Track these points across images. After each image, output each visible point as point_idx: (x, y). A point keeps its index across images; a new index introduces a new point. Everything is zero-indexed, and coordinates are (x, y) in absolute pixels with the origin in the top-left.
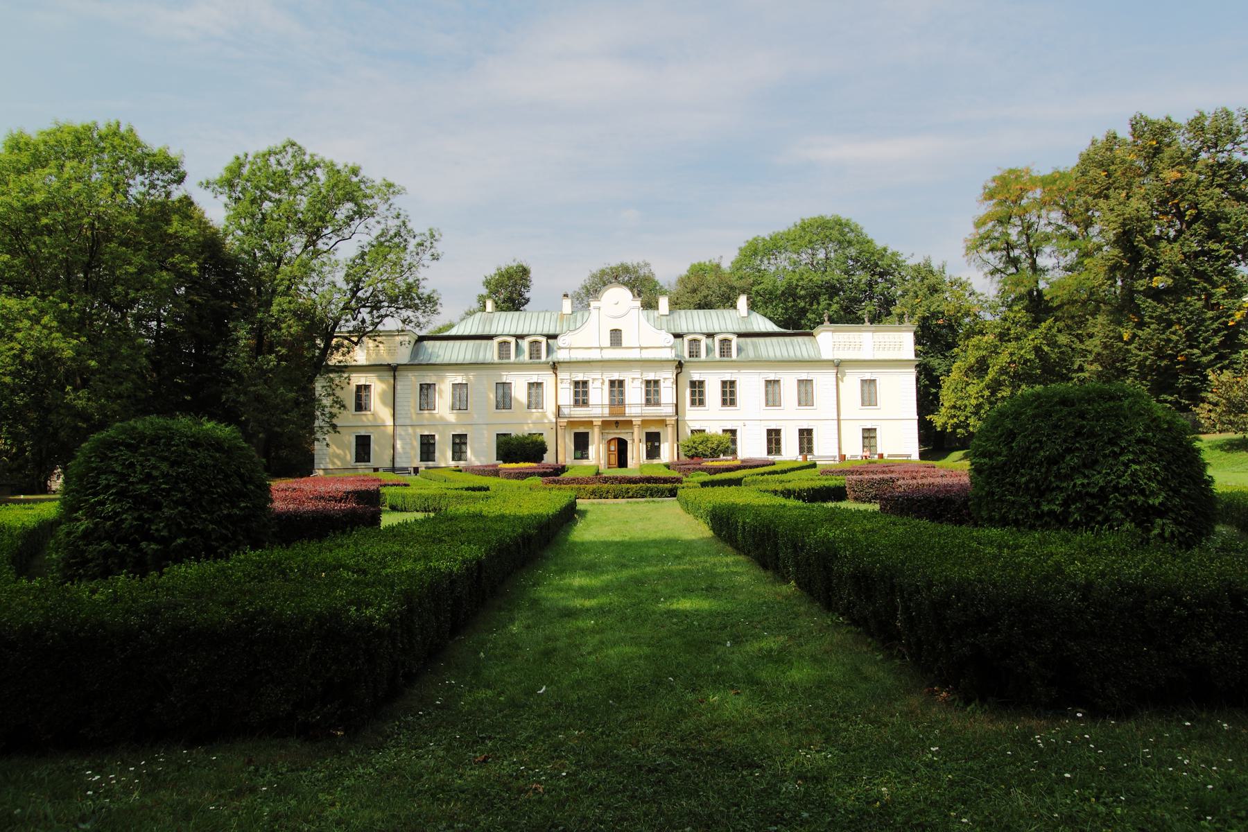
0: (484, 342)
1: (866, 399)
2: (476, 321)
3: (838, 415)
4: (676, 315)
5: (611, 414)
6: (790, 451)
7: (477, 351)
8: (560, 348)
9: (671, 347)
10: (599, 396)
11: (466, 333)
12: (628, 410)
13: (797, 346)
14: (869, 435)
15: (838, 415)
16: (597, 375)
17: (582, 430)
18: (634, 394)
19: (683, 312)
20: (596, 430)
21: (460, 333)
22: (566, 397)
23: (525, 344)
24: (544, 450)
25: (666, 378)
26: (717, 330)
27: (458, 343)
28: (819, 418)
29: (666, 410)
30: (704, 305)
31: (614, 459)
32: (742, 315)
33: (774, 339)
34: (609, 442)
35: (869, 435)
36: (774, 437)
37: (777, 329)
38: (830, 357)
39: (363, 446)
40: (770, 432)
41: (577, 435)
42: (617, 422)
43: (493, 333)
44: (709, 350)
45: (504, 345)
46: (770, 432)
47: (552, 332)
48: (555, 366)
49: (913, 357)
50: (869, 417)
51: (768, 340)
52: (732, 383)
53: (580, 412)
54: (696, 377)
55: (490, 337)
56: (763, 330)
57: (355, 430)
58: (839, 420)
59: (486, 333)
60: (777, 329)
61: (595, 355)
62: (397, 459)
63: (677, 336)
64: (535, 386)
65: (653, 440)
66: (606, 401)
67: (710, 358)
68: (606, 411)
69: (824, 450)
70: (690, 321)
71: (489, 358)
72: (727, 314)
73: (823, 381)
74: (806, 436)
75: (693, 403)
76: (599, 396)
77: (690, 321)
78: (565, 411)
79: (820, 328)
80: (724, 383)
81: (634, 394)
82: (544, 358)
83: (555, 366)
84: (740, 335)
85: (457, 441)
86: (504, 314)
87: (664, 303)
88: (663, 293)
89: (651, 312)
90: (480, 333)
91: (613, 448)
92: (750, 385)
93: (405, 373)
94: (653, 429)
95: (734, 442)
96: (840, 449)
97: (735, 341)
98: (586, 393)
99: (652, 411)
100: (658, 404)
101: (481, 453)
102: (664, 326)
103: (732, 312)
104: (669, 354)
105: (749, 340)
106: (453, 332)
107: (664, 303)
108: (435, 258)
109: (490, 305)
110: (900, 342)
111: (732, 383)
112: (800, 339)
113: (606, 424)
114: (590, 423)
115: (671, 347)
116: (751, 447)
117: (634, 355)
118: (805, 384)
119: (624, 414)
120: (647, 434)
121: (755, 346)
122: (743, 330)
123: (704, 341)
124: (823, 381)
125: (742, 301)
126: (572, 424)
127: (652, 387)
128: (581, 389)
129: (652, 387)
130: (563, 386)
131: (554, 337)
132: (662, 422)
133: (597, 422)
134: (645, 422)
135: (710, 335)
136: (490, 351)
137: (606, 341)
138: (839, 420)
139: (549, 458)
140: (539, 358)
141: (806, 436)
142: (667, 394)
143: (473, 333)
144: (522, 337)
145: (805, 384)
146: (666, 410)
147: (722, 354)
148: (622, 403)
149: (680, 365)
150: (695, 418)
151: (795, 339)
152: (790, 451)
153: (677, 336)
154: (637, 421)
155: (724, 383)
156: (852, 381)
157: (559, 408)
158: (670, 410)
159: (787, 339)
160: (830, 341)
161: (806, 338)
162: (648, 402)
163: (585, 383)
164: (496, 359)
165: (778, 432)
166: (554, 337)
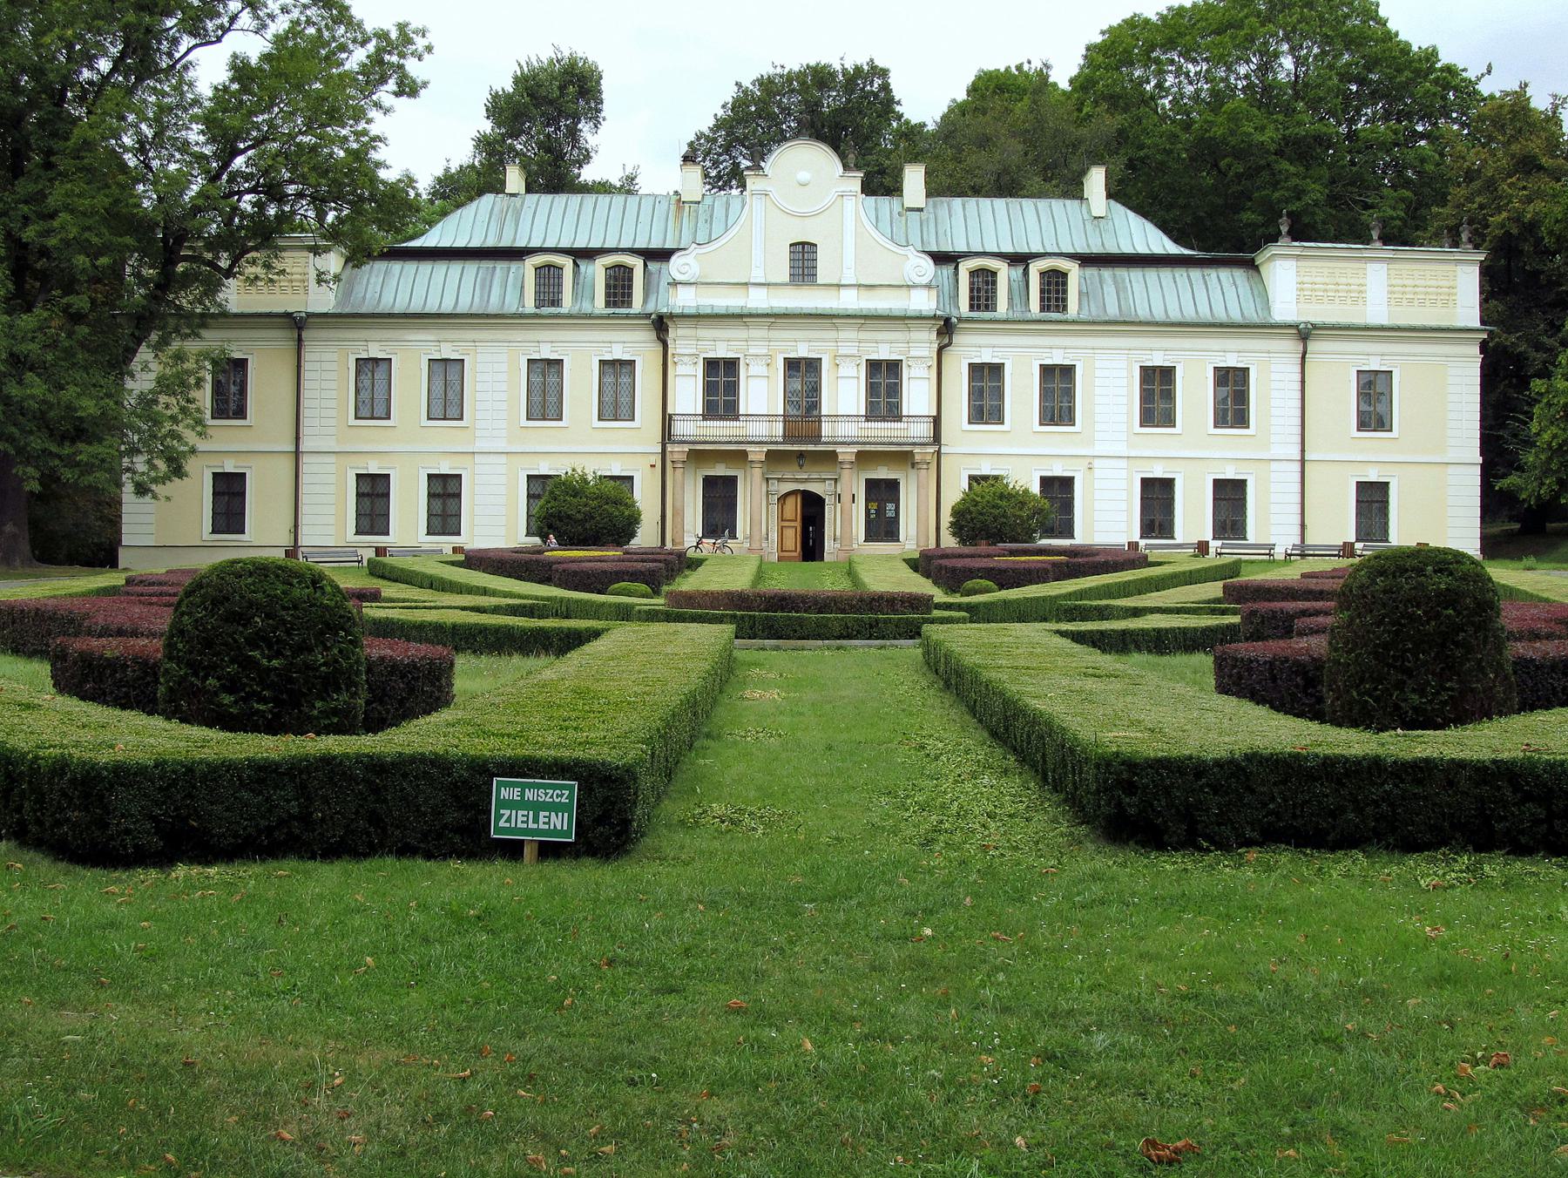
0: (501, 266)
2: (483, 216)
3: (1303, 451)
4: (943, 212)
5: (788, 437)
7: (487, 287)
8: (675, 284)
9: (928, 286)
10: (762, 394)
11: (461, 243)
12: (826, 429)
13: (1218, 291)
14: (1372, 498)
15: (1303, 451)
17: (720, 470)
18: (843, 395)
19: (957, 202)
20: (757, 472)
21: (446, 243)
22: (688, 394)
23: (596, 271)
25: (916, 350)
26: (1036, 248)
27: (441, 268)
28: (1262, 454)
30: (1006, 186)
31: (793, 539)
32: (1097, 216)
33: (1166, 274)
35: (1372, 498)
36: (1157, 497)
37: (1172, 248)
38: (1291, 318)
39: (230, 496)
41: (709, 482)
42: (801, 455)
43: (521, 243)
45: (548, 279)
47: (655, 244)
48: (661, 325)
49: (1477, 324)
50: (1373, 457)
51: (1151, 274)
52: (1068, 371)
53: (720, 430)
54: (987, 357)
56: (1142, 249)
57: (353, 460)
58: (1303, 461)
59: (505, 243)
60: (1172, 248)
61: (758, 300)
62: (303, 530)
63: (940, 258)
64: (617, 370)
65: (883, 493)
67: (1018, 316)
68: (779, 429)
69: (1271, 524)
70: (973, 223)
71: (512, 306)
72: (1060, 209)
74: (1230, 495)
76: (762, 394)
77: (973, 223)
78: (680, 428)
79: (1273, 250)
80: (1047, 371)
81: (843, 395)
82: (637, 304)
83: (661, 325)
84: (1087, 260)
86: (546, 199)
89: (884, 201)
90: (491, 243)
92: (1108, 379)
93: (324, 334)
94: (883, 473)
95: (1067, 506)
97: (1073, 270)
99: (883, 430)
101: (497, 519)
102: (915, 238)
103: (1072, 205)
104: (924, 302)
105: (1107, 273)
106: (431, 240)
107: (914, 178)
108: (409, 88)
109: (514, 178)
110: (1453, 287)
111: (1068, 371)
112: (1225, 274)
114: (740, 457)
115: (928, 286)
116: (1104, 518)
117: (849, 301)
119: (816, 437)
122: (1096, 248)
123: (1004, 272)
124: (1272, 375)
125: (1096, 181)
126: (698, 456)
127: (884, 379)
128: (722, 379)
129: (884, 379)
130: (681, 369)
131: (664, 255)
132: (903, 457)
133: (757, 453)
134: (865, 458)
135: (1019, 260)
136: (515, 287)
137: (781, 269)
138: (1303, 461)
140: (629, 305)
141: (1230, 495)
142: (916, 396)
143: (475, 243)
144: (588, 254)
149: (947, 328)
151: (1212, 274)
153: (940, 258)
154: (846, 453)
155: (1047, 371)
156: (1337, 371)
157: (667, 420)
158: (923, 430)
159: (1196, 273)
160: (1293, 279)
161: (1239, 274)
162: (872, 414)
163: (731, 365)
164: (530, 306)
165: (1167, 485)
166: (664, 255)
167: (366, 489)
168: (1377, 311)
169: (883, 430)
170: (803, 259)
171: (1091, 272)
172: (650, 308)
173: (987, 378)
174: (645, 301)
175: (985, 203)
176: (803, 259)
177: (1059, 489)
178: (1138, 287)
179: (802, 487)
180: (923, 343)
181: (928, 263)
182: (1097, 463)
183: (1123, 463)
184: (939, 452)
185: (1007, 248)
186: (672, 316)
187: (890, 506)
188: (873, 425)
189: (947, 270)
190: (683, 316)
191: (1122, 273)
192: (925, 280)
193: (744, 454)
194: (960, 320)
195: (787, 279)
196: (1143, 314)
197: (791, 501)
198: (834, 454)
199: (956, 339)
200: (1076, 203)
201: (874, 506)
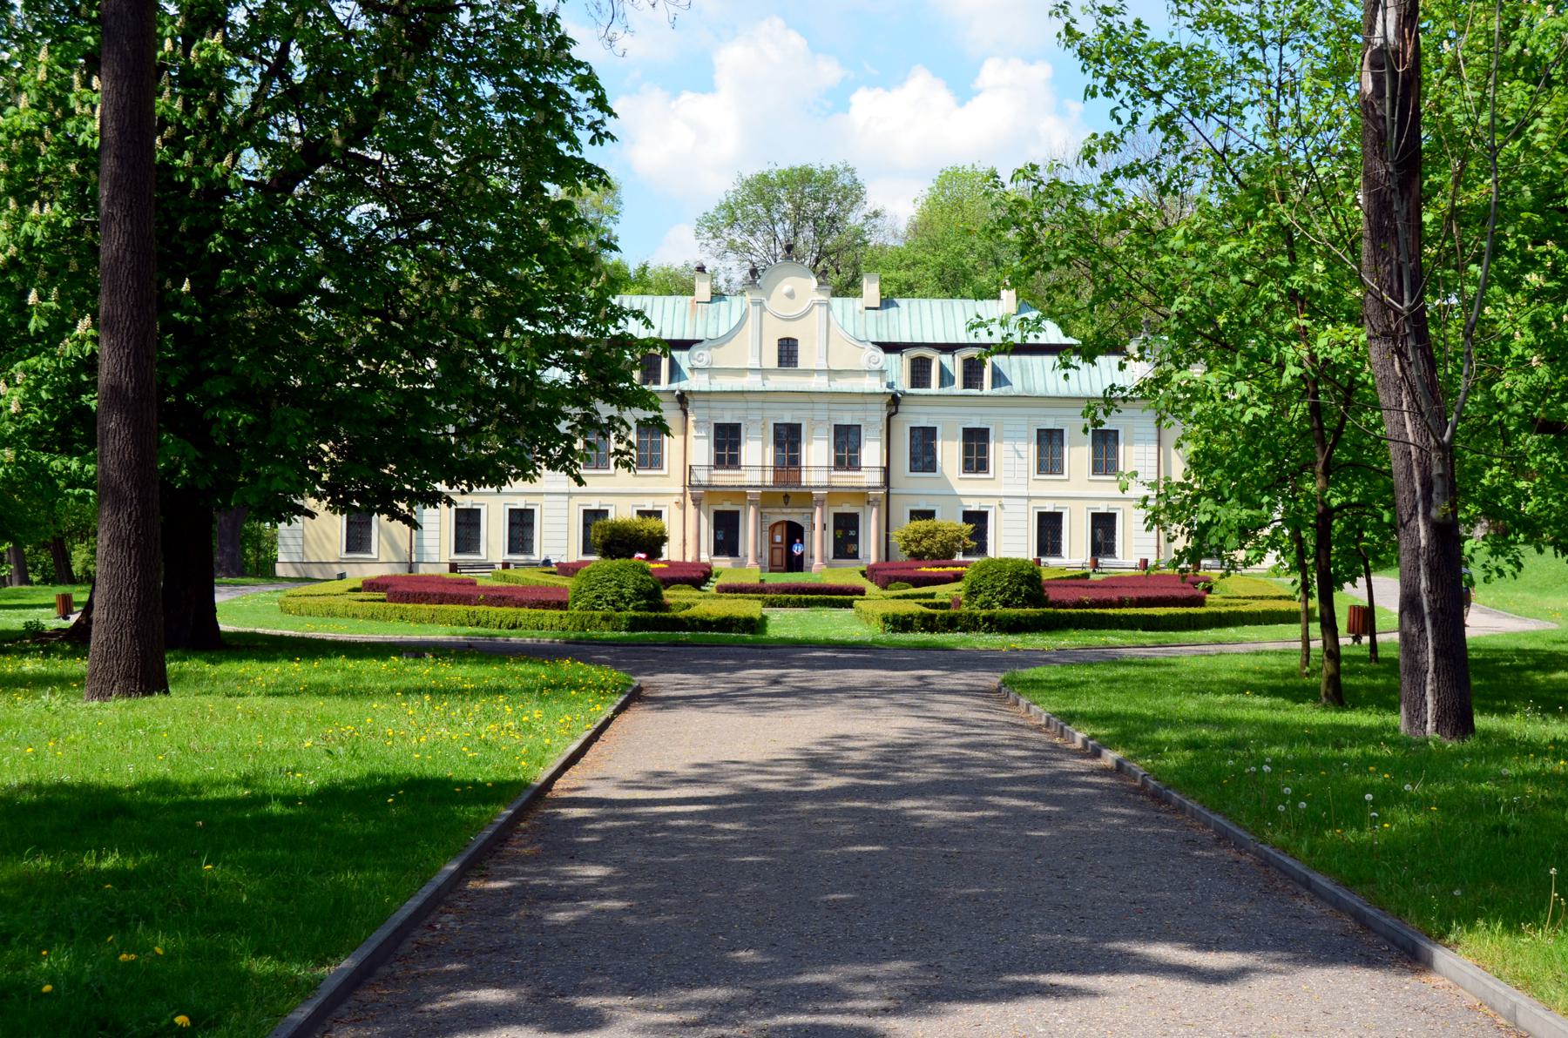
6: (1075, 550)
10: (757, 454)
16: (755, 415)
20: (752, 510)
22: (701, 449)
24: (662, 539)
29: (869, 477)
34: (773, 528)
36: (1049, 528)
40: (1043, 517)
42: (786, 496)
44: (946, 378)
46: (1043, 517)
53: (725, 477)
54: (923, 422)
61: (752, 382)
63: (890, 348)
66: (770, 461)
68: (769, 477)
70: (916, 318)
74: (1103, 525)
76: (757, 454)
77: (916, 318)
81: (816, 453)
82: (664, 385)
83: (682, 399)
85: (517, 520)
87: (871, 290)
88: (874, 265)
89: (848, 301)
91: (778, 539)
94: (847, 509)
98: (736, 444)
99: (845, 478)
105: (1015, 358)
113: (767, 499)
116: (1012, 541)
117: (818, 383)
120: (836, 515)
121: (1023, 370)
128: (727, 440)
132: (861, 495)
134: (834, 493)
137: (771, 360)
139: (671, 552)
141: (1103, 525)
142: (871, 452)
146: (869, 477)
147: (968, 383)
148: (795, 462)
150: (913, 488)
152: (1075, 550)
158: (875, 478)
166: (685, 345)
167: (463, 519)
169: (845, 478)
170: (788, 352)
171: (1001, 360)
172: (674, 386)
173: (924, 441)
174: (670, 381)
175: (925, 302)
176: (788, 352)
177: (978, 520)
178: (1037, 370)
179: (787, 518)
180: (878, 415)
181: (880, 353)
183: (1025, 501)
184: (888, 494)
185: (941, 340)
186: (691, 392)
187: (852, 533)
189: (895, 357)
190: (699, 392)
191: (1026, 359)
192: (877, 367)
193: (745, 494)
194: (904, 394)
196: (1040, 391)
197: (778, 529)
198: (811, 495)
199: (900, 408)
200: (994, 302)
201: (840, 533)
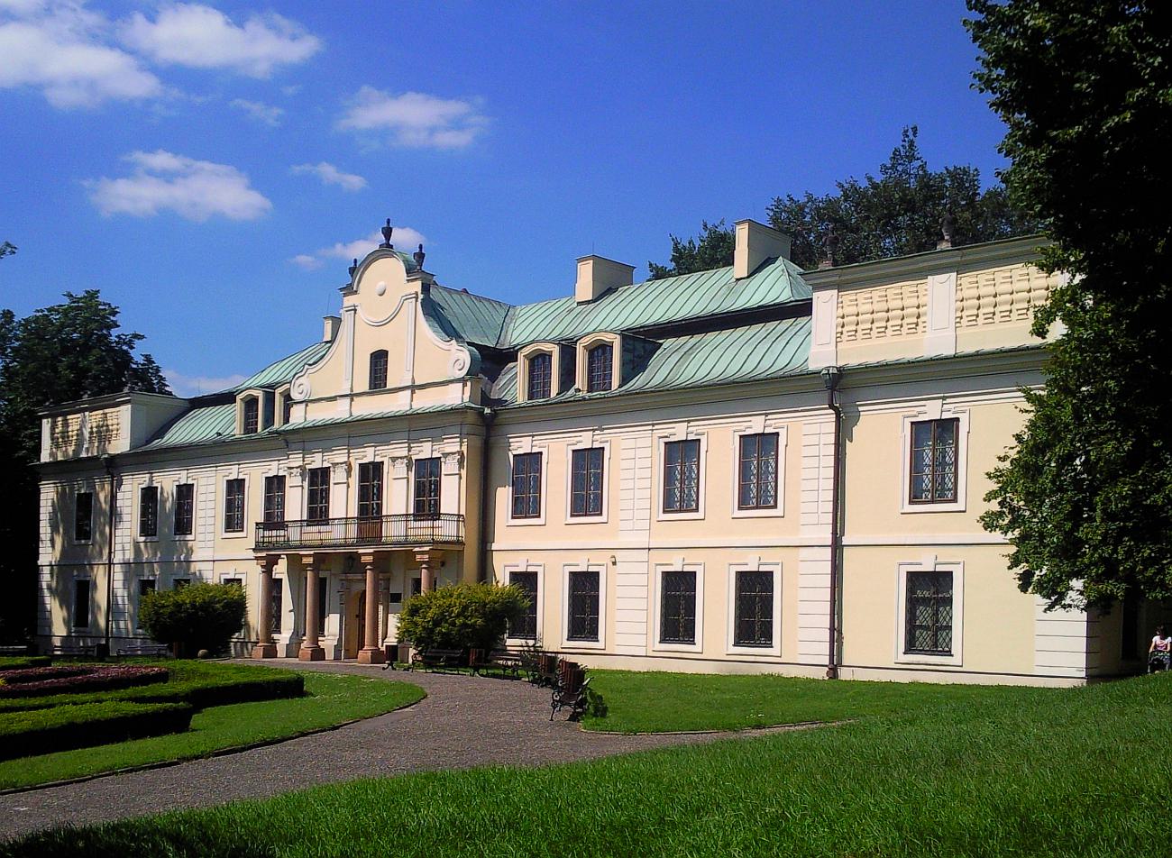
1: (927, 483)
16: (339, 456)
18: (397, 496)
28: (789, 540)
36: (678, 595)
55: (226, 398)
58: (837, 547)
73: (805, 435)
75: (517, 513)
81: (397, 496)
96: (836, 633)
100: (436, 515)
118: (759, 449)
137: (363, 384)
138: (837, 547)
141: (755, 596)
142: (453, 494)
145: (759, 449)
156: (885, 430)
168: (936, 341)
182: (620, 555)
188: (418, 524)
195: (366, 388)
